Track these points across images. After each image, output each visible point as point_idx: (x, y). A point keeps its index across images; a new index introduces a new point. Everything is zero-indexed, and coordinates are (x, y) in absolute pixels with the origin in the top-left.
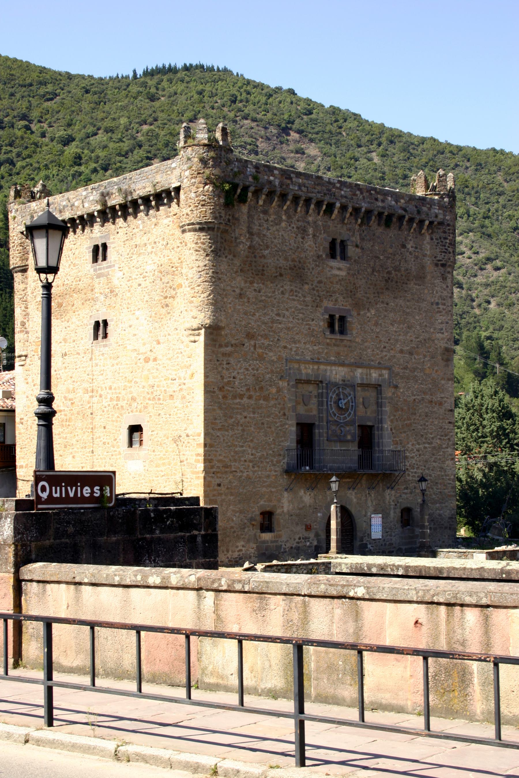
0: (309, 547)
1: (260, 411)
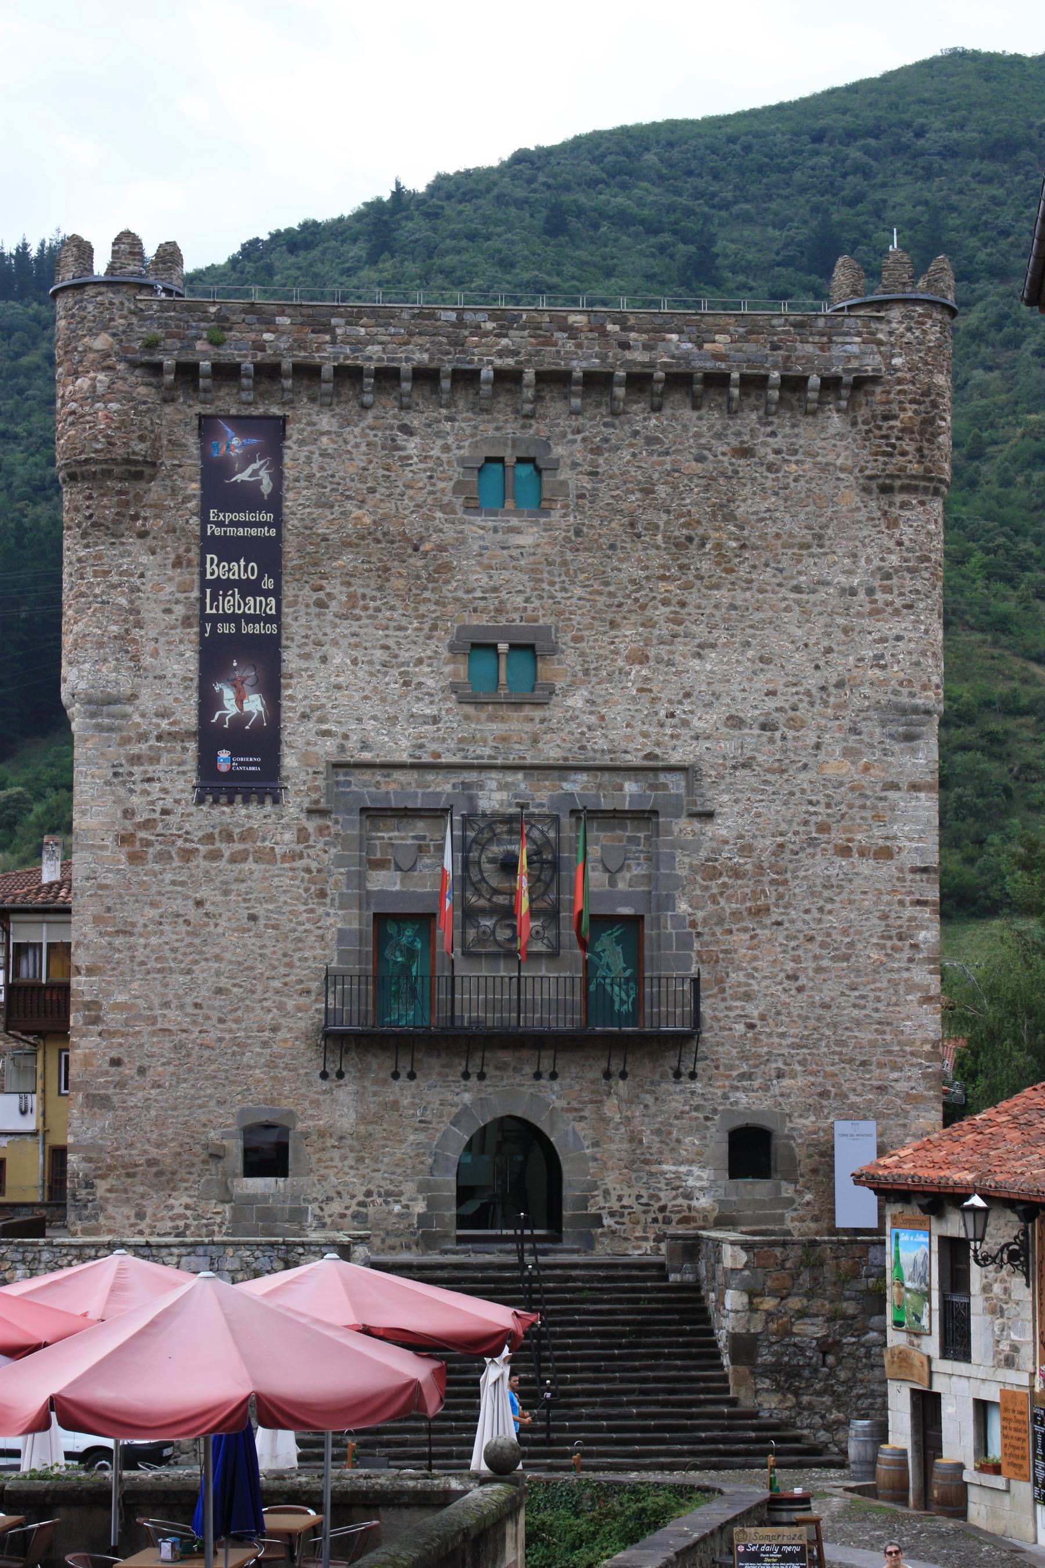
0: (400, 1215)
1: (243, 887)
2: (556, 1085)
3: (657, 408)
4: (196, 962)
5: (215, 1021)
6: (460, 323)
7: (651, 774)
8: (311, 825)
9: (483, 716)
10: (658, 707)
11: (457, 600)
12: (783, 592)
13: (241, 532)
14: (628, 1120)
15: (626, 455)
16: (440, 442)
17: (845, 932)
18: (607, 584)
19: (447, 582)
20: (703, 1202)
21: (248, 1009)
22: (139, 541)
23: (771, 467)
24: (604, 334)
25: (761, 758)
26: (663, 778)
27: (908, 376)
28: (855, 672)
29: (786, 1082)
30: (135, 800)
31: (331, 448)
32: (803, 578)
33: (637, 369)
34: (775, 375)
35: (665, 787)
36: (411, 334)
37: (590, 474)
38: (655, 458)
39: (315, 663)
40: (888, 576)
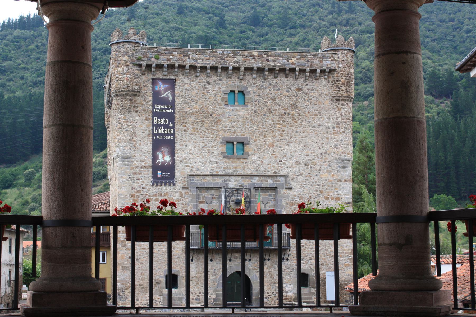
2: (250, 262)
3: (276, 78)
6: (223, 54)
7: (275, 177)
8: (183, 191)
9: (230, 161)
10: (277, 159)
11: (223, 130)
12: (310, 128)
13: (163, 111)
15: (268, 90)
16: (217, 86)
18: (263, 125)
19: (220, 125)
22: (136, 113)
24: (262, 57)
25: (305, 173)
26: (278, 178)
27: (343, 69)
28: (330, 150)
30: (135, 185)
31: (188, 88)
32: (315, 124)
33: (271, 67)
35: (279, 181)
36: (210, 57)
37: (258, 95)
38: (276, 91)
39: (184, 147)
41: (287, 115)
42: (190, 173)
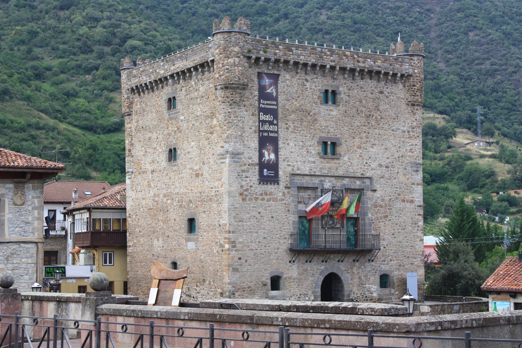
1: (270, 208)
2: (342, 264)
4: (259, 230)
5: (263, 247)
6: (321, 52)
8: (286, 191)
11: (319, 129)
13: (269, 107)
14: (359, 273)
15: (356, 91)
16: (314, 84)
17: (404, 223)
18: (352, 126)
20: (375, 295)
21: (272, 243)
23: (387, 97)
24: (354, 58)
25: (386, 175)
26: (365, 180)
28: (405, 153)
29: (392, 262)
30: (243, 183)
31: (289, 84)
33: (362, 68)
34: (391, 72)
36: (310, 54)
39: (286, 145)
40: (413, 128)
41: (372, 117)
42: (292, 173)
